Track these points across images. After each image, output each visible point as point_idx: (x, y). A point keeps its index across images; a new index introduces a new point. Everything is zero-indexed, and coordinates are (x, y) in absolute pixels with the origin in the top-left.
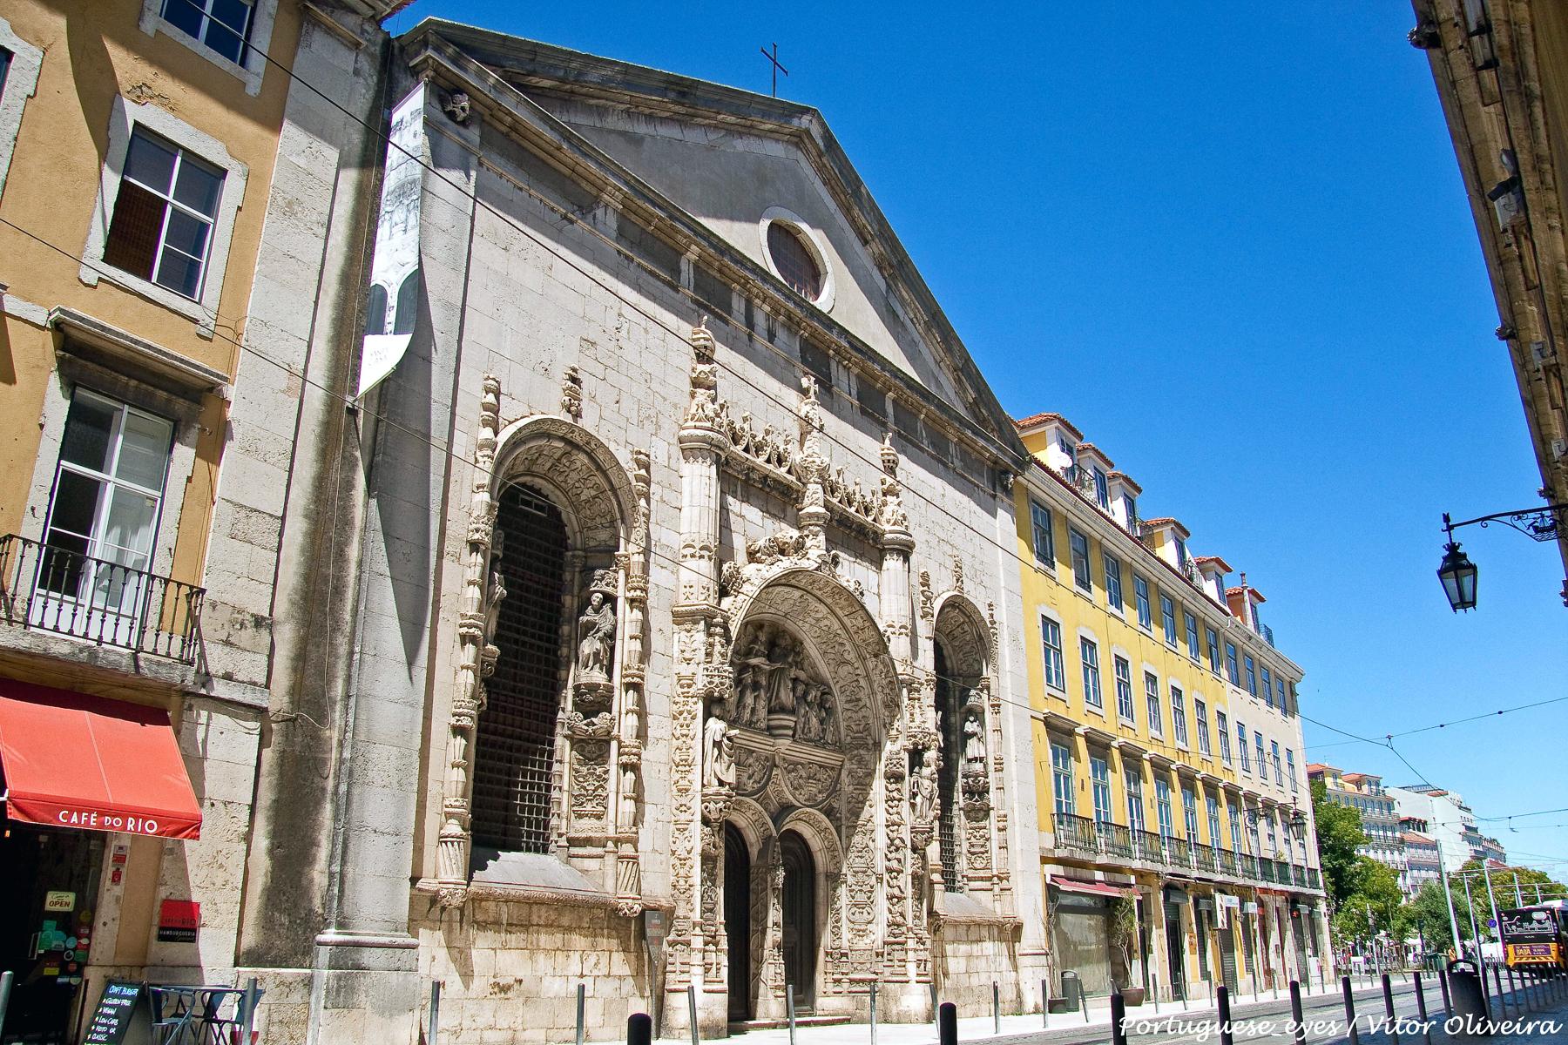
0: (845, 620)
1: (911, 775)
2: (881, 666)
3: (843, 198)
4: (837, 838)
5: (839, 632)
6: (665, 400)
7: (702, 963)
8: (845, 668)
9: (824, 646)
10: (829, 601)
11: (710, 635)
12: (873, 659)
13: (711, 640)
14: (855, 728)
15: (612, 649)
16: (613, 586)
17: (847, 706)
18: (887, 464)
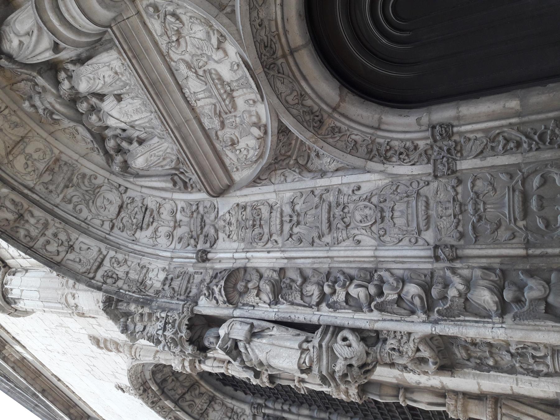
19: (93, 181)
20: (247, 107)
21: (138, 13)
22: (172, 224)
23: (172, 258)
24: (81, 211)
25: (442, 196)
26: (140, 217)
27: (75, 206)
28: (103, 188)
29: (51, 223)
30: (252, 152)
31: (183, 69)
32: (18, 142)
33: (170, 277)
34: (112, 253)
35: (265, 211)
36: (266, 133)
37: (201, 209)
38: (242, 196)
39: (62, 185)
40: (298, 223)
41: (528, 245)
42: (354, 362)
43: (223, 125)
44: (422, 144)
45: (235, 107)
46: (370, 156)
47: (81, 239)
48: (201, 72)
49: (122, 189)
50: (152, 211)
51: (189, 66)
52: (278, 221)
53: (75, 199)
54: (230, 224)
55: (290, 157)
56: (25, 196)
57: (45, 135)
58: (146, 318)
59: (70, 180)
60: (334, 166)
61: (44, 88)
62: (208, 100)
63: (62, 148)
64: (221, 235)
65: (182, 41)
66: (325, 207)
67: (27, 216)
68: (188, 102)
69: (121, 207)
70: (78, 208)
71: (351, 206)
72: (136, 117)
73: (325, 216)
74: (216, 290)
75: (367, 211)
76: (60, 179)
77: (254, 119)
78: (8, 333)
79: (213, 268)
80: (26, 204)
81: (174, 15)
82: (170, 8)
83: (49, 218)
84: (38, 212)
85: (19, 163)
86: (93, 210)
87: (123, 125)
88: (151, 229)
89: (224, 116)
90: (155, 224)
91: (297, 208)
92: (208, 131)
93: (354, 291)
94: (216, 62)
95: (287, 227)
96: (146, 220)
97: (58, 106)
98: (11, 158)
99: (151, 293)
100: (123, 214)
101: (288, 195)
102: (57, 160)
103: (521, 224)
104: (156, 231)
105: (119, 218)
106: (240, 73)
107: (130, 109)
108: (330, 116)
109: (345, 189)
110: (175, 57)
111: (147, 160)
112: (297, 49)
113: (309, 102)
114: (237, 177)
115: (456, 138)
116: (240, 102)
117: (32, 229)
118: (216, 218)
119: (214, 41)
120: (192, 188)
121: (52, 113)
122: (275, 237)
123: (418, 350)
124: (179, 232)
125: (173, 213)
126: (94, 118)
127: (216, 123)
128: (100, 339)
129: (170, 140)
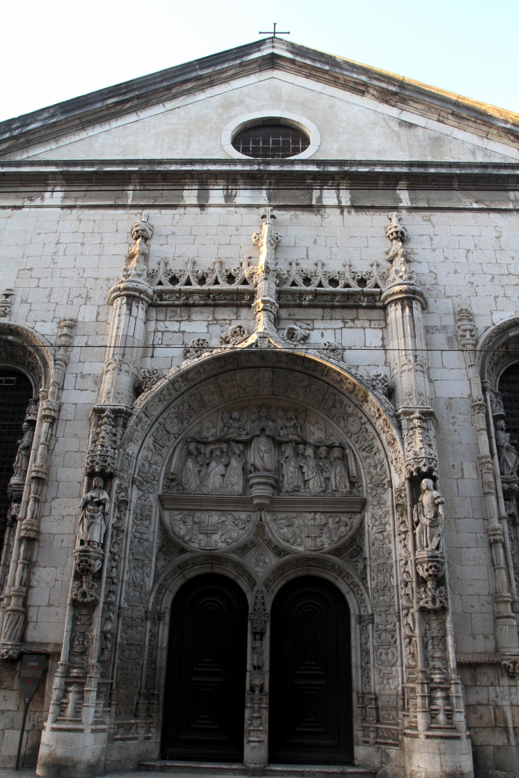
0: (324, 378)
1: (412, 506)
2: (372, 408)
3: (326, 76)
4: (357, 580)
5: (331, 391)
6: (97, 279)
7: (57, 703)
8: (351, 419)
9: (326, 407)
10: (299, 368)
11: (98, 426)
12: (365, 404)
13: (98, 430)
14: (374, 472)
15: (28, 457)
16: (34, 415)
17: (364, 454)
18: (391, 237)
19: (186, 421)
20: (199, 539)
21: (250, 511)
22: (152, 462)
23: (137, 459)
24: (175, 408)
25: (139, 613)
26: (160, 442)
27: (179, 407)
28: (180, 424)
29: (177, 393)
30: (178, 529)
31: (223, 519)
32: (222, 393)
33: (129, 458)
34: (149, 422)
35: (146, 523)
36: (185, 542)
37: (154, 482)
38: (156, 511)
39: (192, 404)
40: (139, 542)
41: (120, 644)
42: (92, 568)
43: (195, 522)
44: (158, 607)
45: (201, 533)
46: (161, 586)
47: (162, 406)
48: (219, 525)
49: (177, 436)
50: (161, 450)
51: (223, 522)
52: (142, 531)
53: (181, 407)
54: (145, 500)
55: (167, 544)
56: (195, 385)
57: (219, 407)
58: (114, 438)
59: (193, 409)
60: (158, 565)
61: (240, 435)
62: (207, 521)
63: (209, 413)
64: (141, 493)
65: (233, 524)
66: (143, 558)
67: (186, 383)
68: (210, 510)
69: (168, 432)
70: (177, 407)
71: (141, 571)
72: (212, 480)
73: (140, 557)
74: (124, 494)
75: (139, 579)
76: (195, 405)
77: (193, 540)
78: (82, 207)
79: (128, 487)
80: (192, 384)
81: (243, 528)
82: (246, 528)
83: (179, 393)
84: (184, 389)
85: (212, 388)
86: (173, 415)
87: (210, 469)
88: (151, 446)
89: (198, 525)
90: (154, 450)
91: (145, 543)
92: (193, 512)
93: (114, 570)
94: (221, 536)
95: (138, 535)
96: (158, 446)
97: (230, 436)
98: (217, 385)
99: (125, 446)
100: (165, 432)
101: (151, 539)
102: (205, 406)
103: (125, 642)
104: (151, 450)
105: (163, 429)
106: (213, 544)
107: (216, 480)
108: (182, 573)
109: (149, 569)
110: (229, 517)
111: (190, 470)
112: (212, 567)
113: (190, 566)
114: (167, 513)
115: (157, 622)
116: (201, 537)
117: (179, 384)
118: (149, 492)
119: (229, 540)
120: (167, 482)
121: (228, 427)
122: (135, 527)
123: (91, 596)
124: (147, 465)
125: (156, 463)
126: (218, 454)
127: (196, 520)
128: (73, 331)
129: (197, 492)
